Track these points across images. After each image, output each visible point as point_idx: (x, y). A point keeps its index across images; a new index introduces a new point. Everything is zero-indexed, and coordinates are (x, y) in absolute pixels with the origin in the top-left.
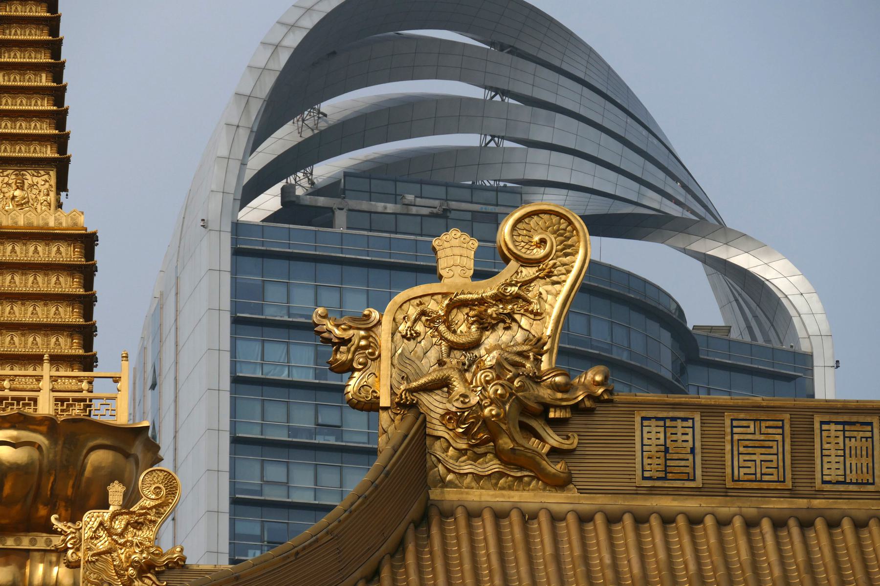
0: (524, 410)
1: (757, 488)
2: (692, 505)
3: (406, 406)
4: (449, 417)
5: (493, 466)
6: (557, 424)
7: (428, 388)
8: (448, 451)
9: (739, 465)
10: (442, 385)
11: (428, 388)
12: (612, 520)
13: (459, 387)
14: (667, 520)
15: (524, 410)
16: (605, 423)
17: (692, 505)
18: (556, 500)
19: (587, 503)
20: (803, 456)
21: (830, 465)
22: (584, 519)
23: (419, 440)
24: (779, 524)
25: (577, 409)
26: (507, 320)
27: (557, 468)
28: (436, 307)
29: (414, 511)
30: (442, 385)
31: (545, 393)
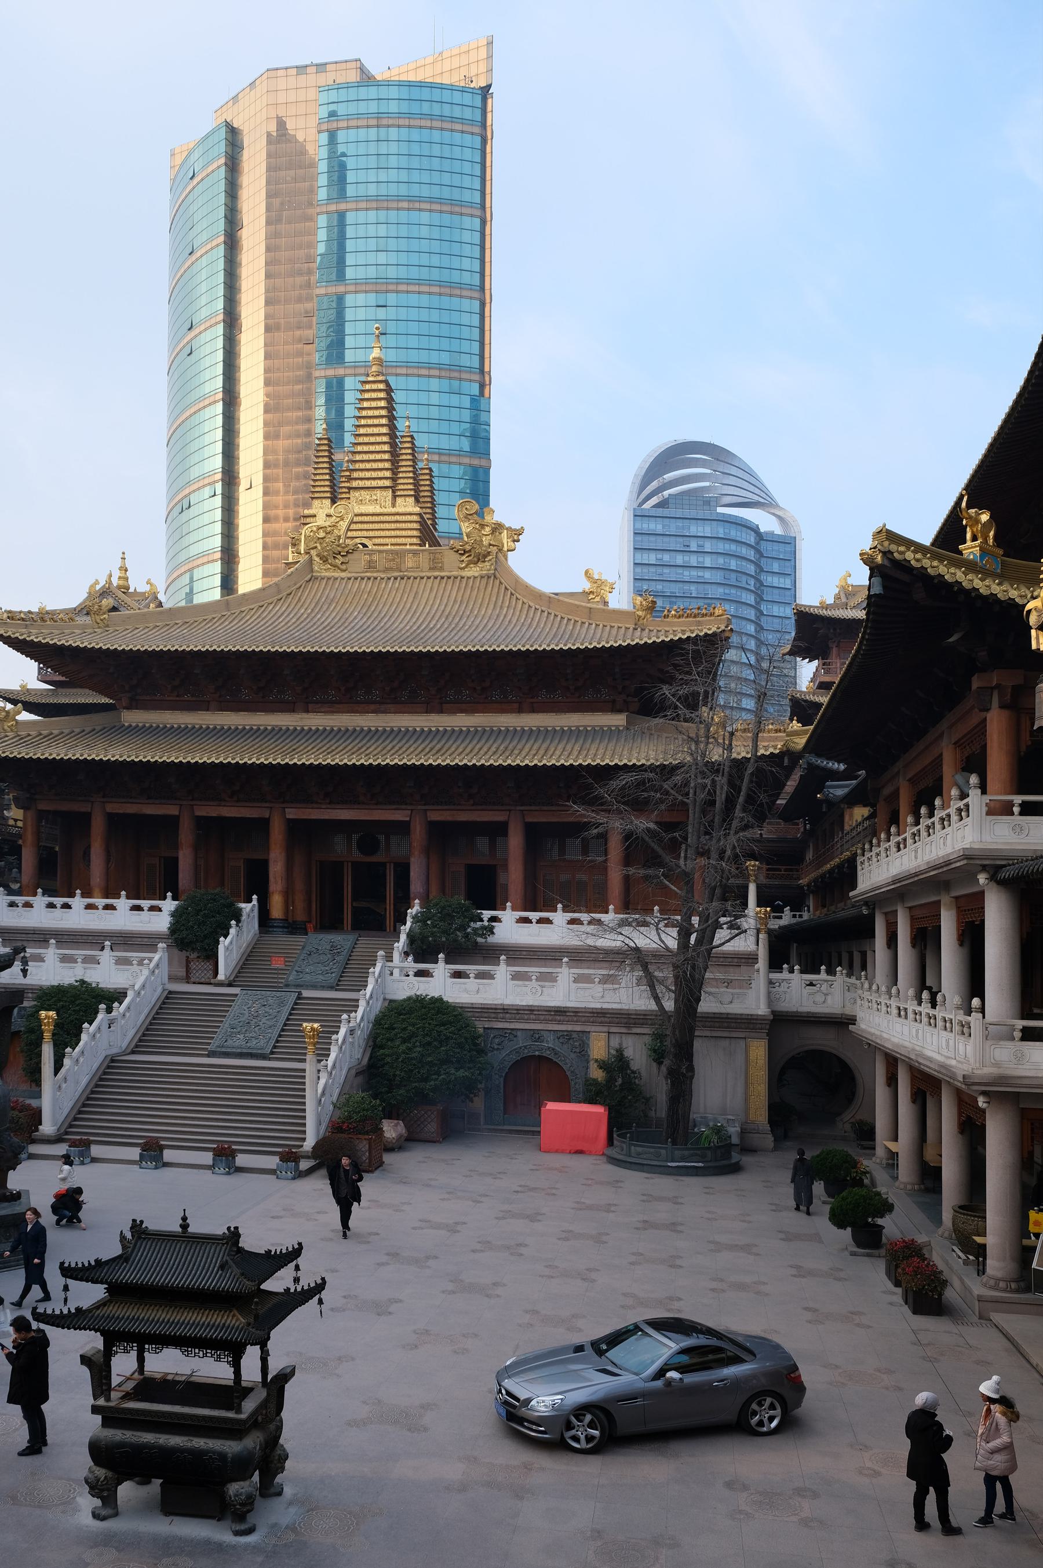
19: (349, 575)
31: (339, 549)
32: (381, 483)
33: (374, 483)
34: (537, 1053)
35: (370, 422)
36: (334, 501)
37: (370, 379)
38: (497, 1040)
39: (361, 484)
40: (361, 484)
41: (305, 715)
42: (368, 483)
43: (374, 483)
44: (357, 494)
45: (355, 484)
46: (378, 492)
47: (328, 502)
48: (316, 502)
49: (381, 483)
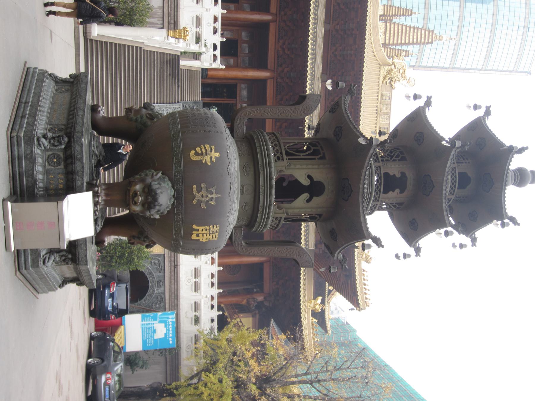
0: (392, 78)
1: (381, 107)
2: (379, 99)
3: (393, 63)
4: (391, 69)
5: (386, 74)
6: (390, 82)
7: (395, 66)
8: (387, 68)
9: (384, 106)
10: (395, 68)
11: (395, 66)
12: (378, 89)
13: (395, 70)
14: (378, 96)
15: (392, 78)
16: (391, 88)
17: (379, 99)
18: (381, 82)
20: (384, 113)
21: (383, 117)
22: (378, 86)
23: (389, 65)
24: (377, 110)
25: (392, 85)
26: (402, 77)
27: (385, 81)
28: (404, 68)
29: (381, 63)
30: (395, 68)
32: (387, 38)
33: (388, 35)
34: (150, 284)
35: (415, 34)
36: (381, 16)
37: (434, 35)
38: (157, 262)
39: (388, 28)
40: (388, 28)
41: (320, 81)
42: (388, 32)
43: (388, 35)
44: (383, 26)
45: (388, 25)
46: (384, 37)
47: (382, 13)
48: (383, 7)
49: (387, 38)
